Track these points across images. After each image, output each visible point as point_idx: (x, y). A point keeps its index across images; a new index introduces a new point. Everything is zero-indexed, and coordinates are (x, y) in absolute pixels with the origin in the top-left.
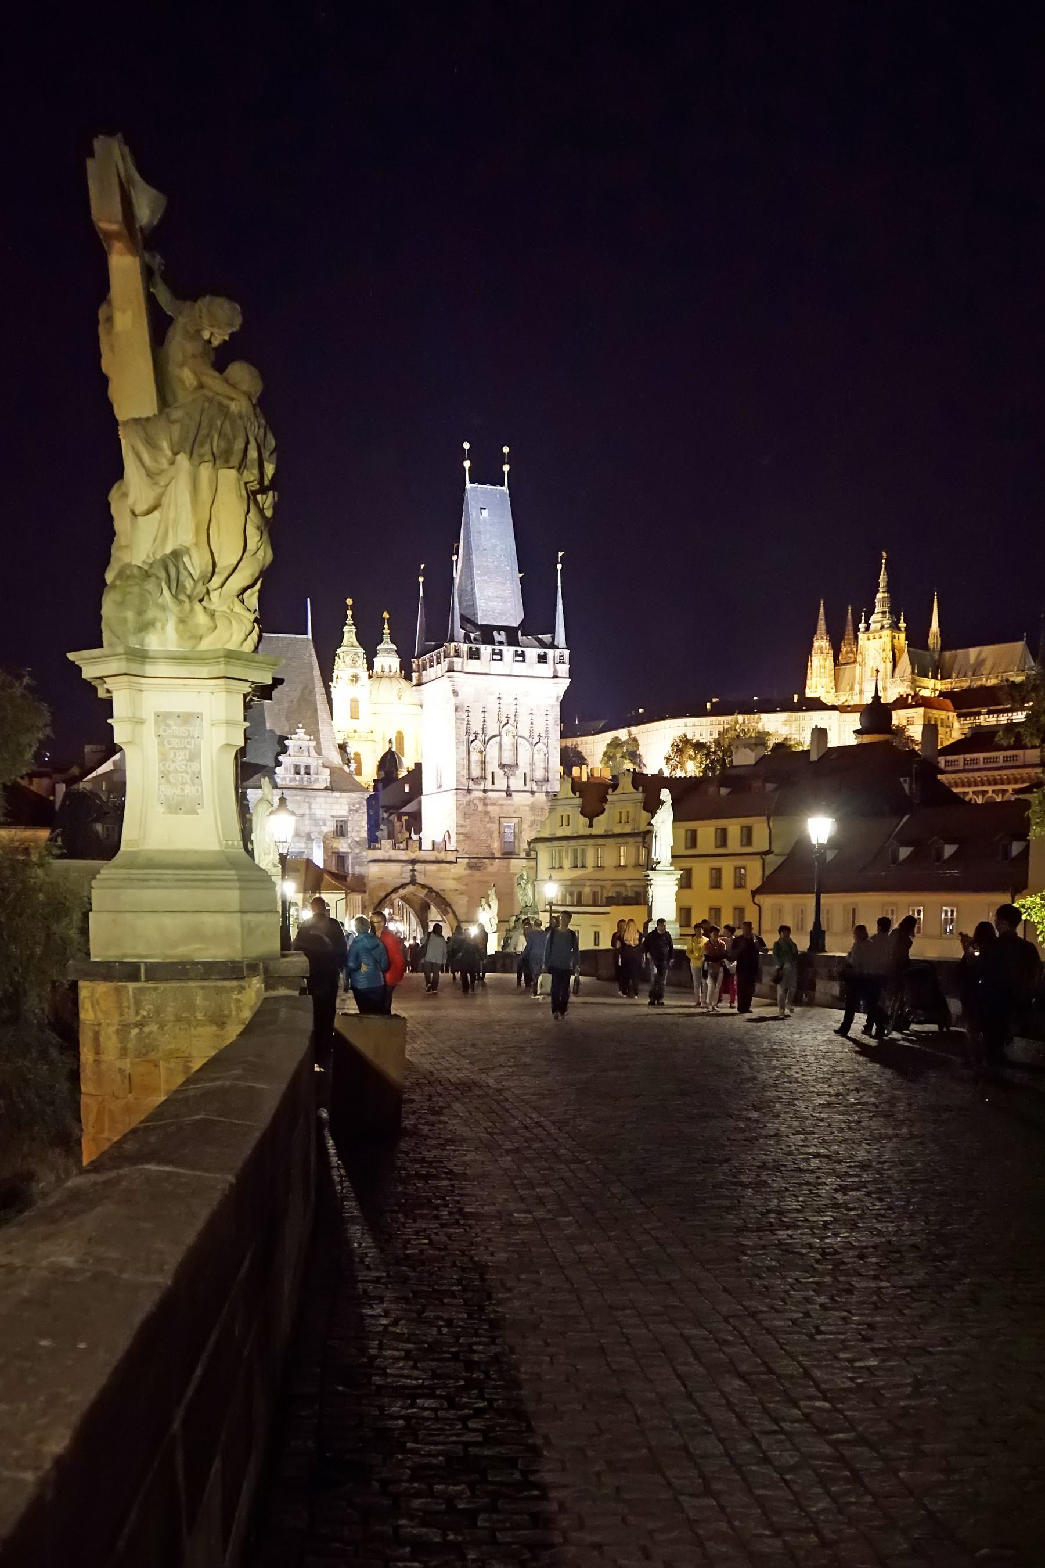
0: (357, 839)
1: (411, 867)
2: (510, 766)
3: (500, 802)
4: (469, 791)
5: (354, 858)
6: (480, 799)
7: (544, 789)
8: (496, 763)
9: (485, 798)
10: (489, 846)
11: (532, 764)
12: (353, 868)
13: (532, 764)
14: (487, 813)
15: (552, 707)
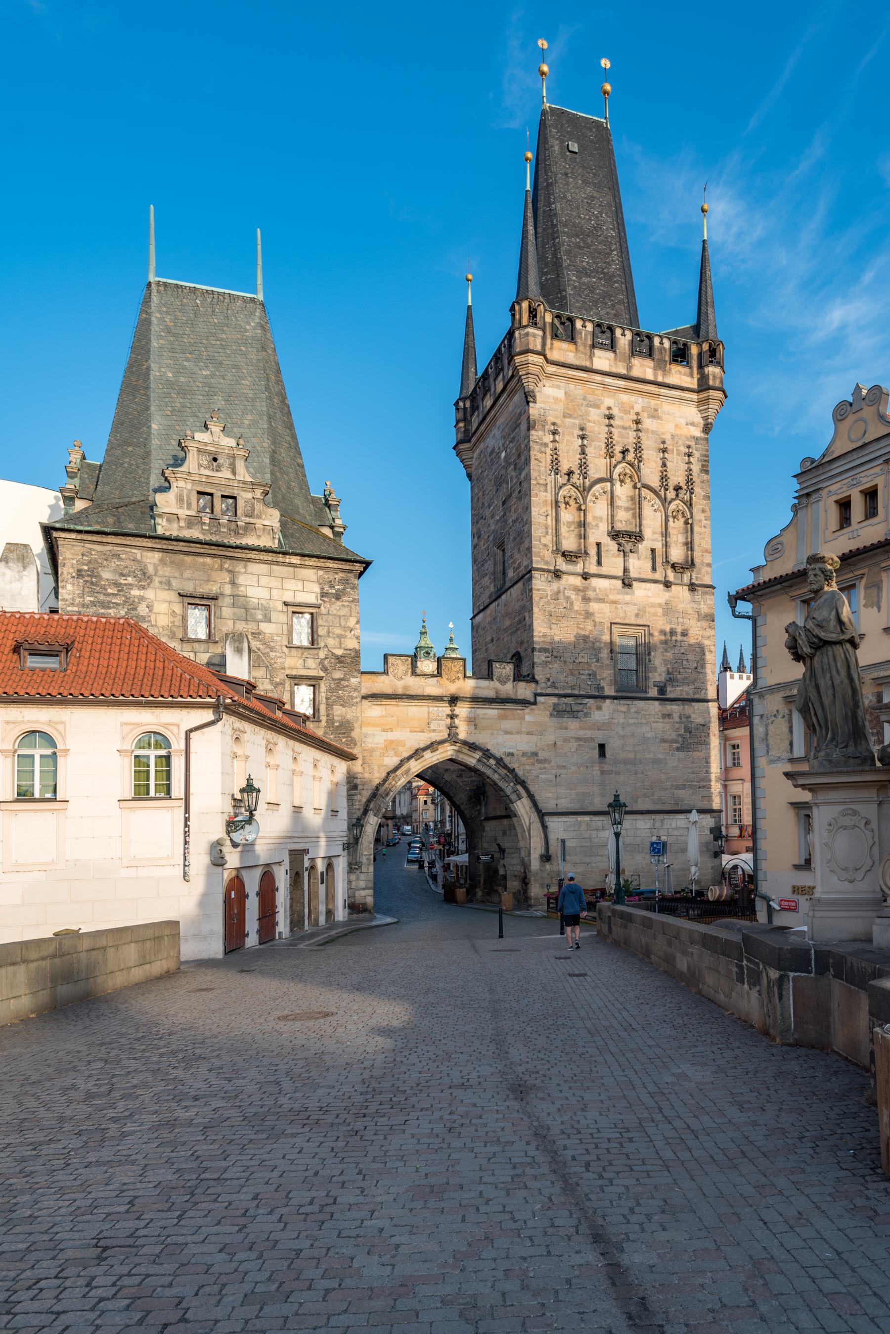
0: (339, 652)
1: (447, 710)
2: (629, 535)
3: (612, 597)
4: (557, 574)
5: (330, 690)
6: (576, 589)
7: (686, 578)
8: (604, 527)
9: (585, 589)
10: (593, 675)
11: (666, 534)
12: (329, 706)
13: (666, 534)
14: (588, 615)
15: (697, 440)
